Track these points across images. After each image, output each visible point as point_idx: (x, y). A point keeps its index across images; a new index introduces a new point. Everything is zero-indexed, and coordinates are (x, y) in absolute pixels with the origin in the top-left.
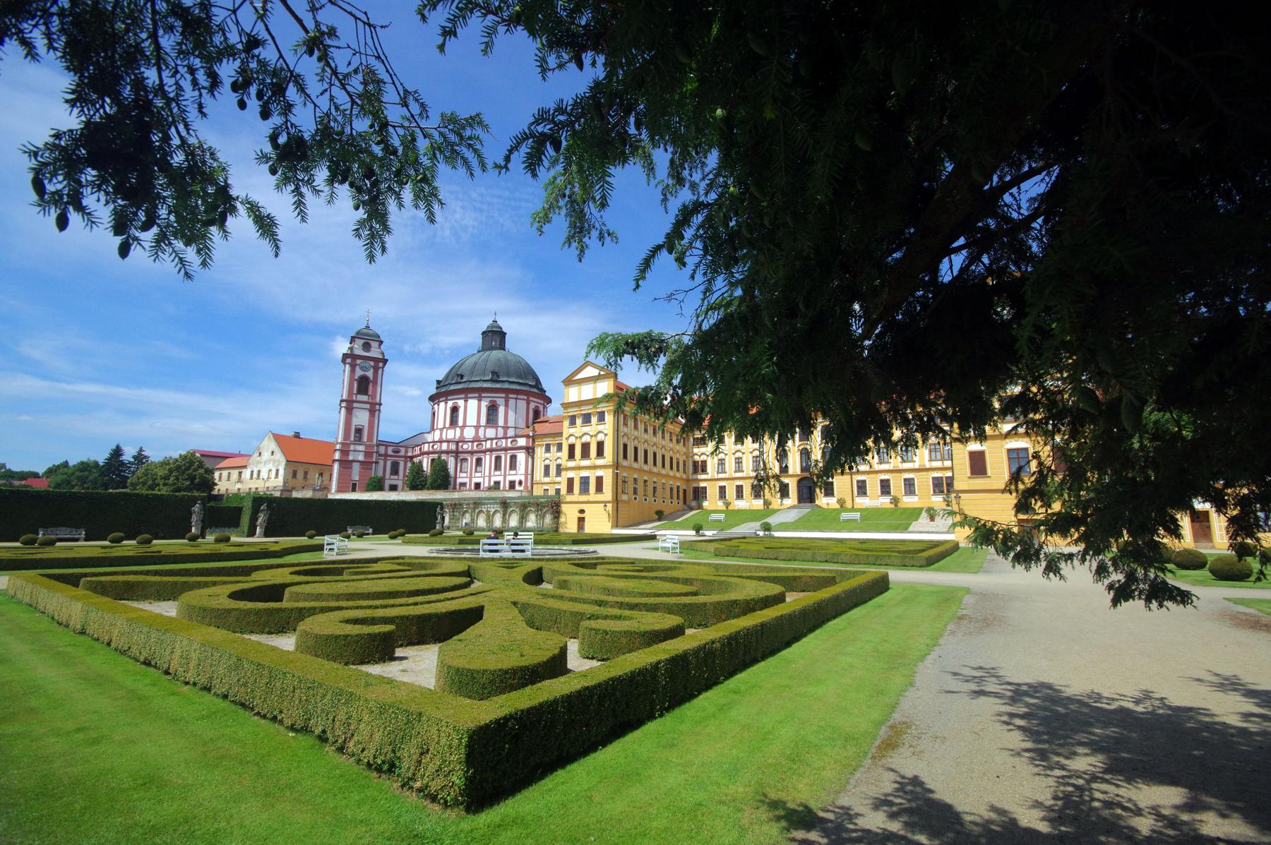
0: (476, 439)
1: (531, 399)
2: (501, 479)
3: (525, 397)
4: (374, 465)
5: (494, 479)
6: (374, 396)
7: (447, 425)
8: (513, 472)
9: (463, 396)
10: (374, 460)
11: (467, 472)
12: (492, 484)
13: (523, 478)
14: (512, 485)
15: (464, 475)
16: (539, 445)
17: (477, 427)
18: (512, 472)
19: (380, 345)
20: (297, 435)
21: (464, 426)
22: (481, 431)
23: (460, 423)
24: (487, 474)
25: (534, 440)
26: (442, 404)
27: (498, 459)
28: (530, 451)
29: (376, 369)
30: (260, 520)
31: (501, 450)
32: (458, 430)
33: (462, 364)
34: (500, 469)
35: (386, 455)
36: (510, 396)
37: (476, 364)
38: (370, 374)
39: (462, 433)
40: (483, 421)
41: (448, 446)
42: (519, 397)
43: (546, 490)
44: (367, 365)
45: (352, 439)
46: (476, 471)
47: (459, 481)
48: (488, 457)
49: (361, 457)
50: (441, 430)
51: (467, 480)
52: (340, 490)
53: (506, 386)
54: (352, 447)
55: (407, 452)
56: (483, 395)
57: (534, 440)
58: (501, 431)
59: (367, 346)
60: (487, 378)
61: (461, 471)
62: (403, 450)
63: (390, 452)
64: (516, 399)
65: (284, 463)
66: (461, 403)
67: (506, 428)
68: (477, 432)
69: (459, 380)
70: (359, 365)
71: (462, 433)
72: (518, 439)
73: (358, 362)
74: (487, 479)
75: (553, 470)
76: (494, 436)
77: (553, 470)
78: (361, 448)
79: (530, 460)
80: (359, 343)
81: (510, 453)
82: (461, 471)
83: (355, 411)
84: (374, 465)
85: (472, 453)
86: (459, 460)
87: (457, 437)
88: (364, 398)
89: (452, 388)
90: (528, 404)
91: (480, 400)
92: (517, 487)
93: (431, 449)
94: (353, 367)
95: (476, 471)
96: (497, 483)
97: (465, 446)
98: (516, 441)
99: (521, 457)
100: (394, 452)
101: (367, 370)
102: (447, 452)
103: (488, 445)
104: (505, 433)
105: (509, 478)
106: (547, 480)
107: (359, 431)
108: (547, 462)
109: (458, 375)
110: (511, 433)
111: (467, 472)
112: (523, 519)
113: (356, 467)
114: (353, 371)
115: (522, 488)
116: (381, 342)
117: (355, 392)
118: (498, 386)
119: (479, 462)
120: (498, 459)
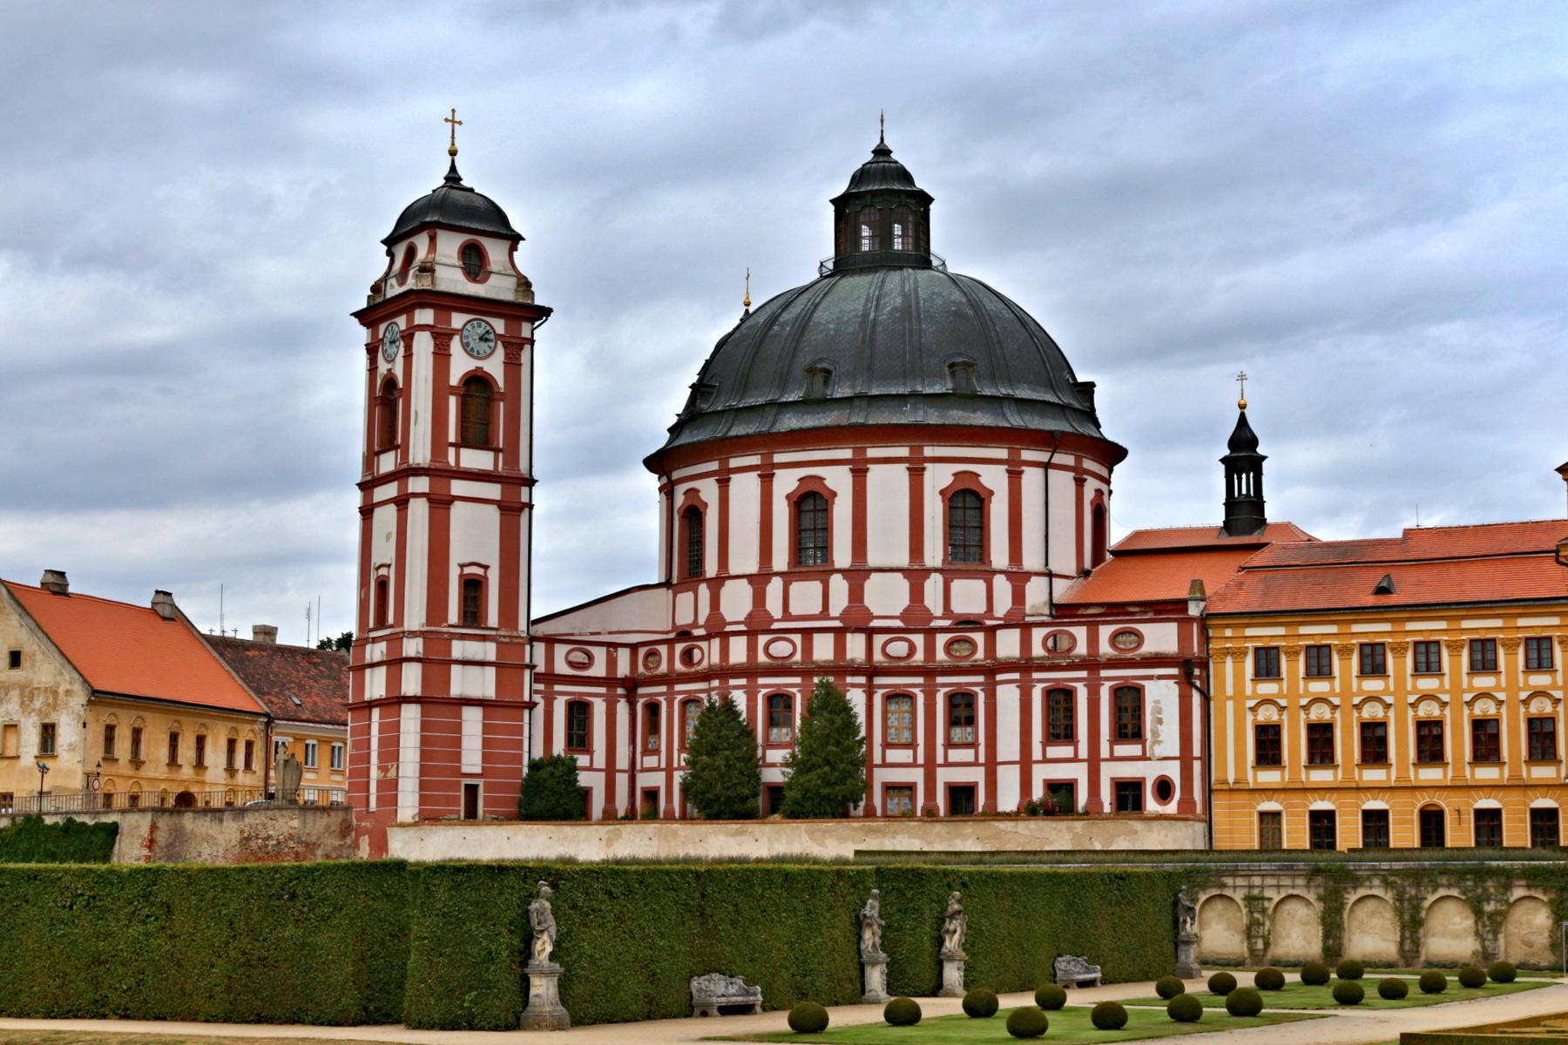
0: (915, 619)
1: (1088, 464)
2: (1079, 773)
3: (1069, 460)
4: (526, 712)
6: (511, 452)
7: (781, 561)
8: (1134, 749)
9: (847, 454)
10: (526, 698)
11: (912, 745)
12: (1038, 793)
13: (1173, 771)
14: (1129, 795)
15: (904, 755)
16: (1227, 652)
17: (916, 575)
18: (1122, 750)
19: (513, 248)
20: (56, 584)
21: (858, 575)
22: (933, 586)
23: (842, 556)
24: (1009, 747)
25: (1206, 639)
26: (745, 488)
27: (1060, 700)
29: (517, 347)
30: (952, 943)
32: (839, 585)
33: (804, 323)
35: (550, 678)
36: (1027, 455)
37: (868, 326)
38: (495, 367)
39: (856, 594)
40: (934, 553)
41: (840, 648)
42: (1060, 458)
43: (1270, 820)
45: (453, 615)
46: (950, 744)
47: (881, 776)
48: (1008, 695)
49: (483, 684)
50: (759, 580)
51: (917, 776)
52: (429, 817)
53: (1015, 420)
55: (612, 663)
56: (929, 451)
57: (1206, 639)
58: (1002, 586)
59: (474, 262)
60: (937, 389)
61: (887, 745)
62: (600, 654)
63: (561, 668)
64: (1047, 466)
65: (80, 697)
66: (839, 480)
67: (1019, 578)
68: (917, 594)
69: (818, 391)
70: (459, 332)
71: (856, 594)
73: (458, 320)
74: (1009, 779)
75: (1295, 744)
76: (979, 608)
77: (1295, 744)
78: (489, 651)
79: (1196, 698)
80: (449, 246)
81: (1111, 676)
82: (887, 745)
83: (457, 510)
84: (526, 712)
85: (929, 672)
86: (878, 699)
87: (836, 609)
89: (791, 422)
90: (1080, 483)
92: (1151, 805)
94: (442, 339)
95: (950, 744)
96: (1061, 791)
97: (898, 649)
99: (1161, 695)
100: (571, 664)
102: (841, 668)
103: (1008, 644)
104: (1019, 597)
106: (1270, 777)
107: (473, 587)
108: (1268, 715)
109: (811, 371)
110: (1036, 593)
111: (912, 745)
112: (1412, 924)
113: (472, 719)
114: (441, 356)
115: (1172, 808)
116: (515, 239)
117: (452, 438)
118: (981, 419)
119: (961, 710)
120: (1060, 700)
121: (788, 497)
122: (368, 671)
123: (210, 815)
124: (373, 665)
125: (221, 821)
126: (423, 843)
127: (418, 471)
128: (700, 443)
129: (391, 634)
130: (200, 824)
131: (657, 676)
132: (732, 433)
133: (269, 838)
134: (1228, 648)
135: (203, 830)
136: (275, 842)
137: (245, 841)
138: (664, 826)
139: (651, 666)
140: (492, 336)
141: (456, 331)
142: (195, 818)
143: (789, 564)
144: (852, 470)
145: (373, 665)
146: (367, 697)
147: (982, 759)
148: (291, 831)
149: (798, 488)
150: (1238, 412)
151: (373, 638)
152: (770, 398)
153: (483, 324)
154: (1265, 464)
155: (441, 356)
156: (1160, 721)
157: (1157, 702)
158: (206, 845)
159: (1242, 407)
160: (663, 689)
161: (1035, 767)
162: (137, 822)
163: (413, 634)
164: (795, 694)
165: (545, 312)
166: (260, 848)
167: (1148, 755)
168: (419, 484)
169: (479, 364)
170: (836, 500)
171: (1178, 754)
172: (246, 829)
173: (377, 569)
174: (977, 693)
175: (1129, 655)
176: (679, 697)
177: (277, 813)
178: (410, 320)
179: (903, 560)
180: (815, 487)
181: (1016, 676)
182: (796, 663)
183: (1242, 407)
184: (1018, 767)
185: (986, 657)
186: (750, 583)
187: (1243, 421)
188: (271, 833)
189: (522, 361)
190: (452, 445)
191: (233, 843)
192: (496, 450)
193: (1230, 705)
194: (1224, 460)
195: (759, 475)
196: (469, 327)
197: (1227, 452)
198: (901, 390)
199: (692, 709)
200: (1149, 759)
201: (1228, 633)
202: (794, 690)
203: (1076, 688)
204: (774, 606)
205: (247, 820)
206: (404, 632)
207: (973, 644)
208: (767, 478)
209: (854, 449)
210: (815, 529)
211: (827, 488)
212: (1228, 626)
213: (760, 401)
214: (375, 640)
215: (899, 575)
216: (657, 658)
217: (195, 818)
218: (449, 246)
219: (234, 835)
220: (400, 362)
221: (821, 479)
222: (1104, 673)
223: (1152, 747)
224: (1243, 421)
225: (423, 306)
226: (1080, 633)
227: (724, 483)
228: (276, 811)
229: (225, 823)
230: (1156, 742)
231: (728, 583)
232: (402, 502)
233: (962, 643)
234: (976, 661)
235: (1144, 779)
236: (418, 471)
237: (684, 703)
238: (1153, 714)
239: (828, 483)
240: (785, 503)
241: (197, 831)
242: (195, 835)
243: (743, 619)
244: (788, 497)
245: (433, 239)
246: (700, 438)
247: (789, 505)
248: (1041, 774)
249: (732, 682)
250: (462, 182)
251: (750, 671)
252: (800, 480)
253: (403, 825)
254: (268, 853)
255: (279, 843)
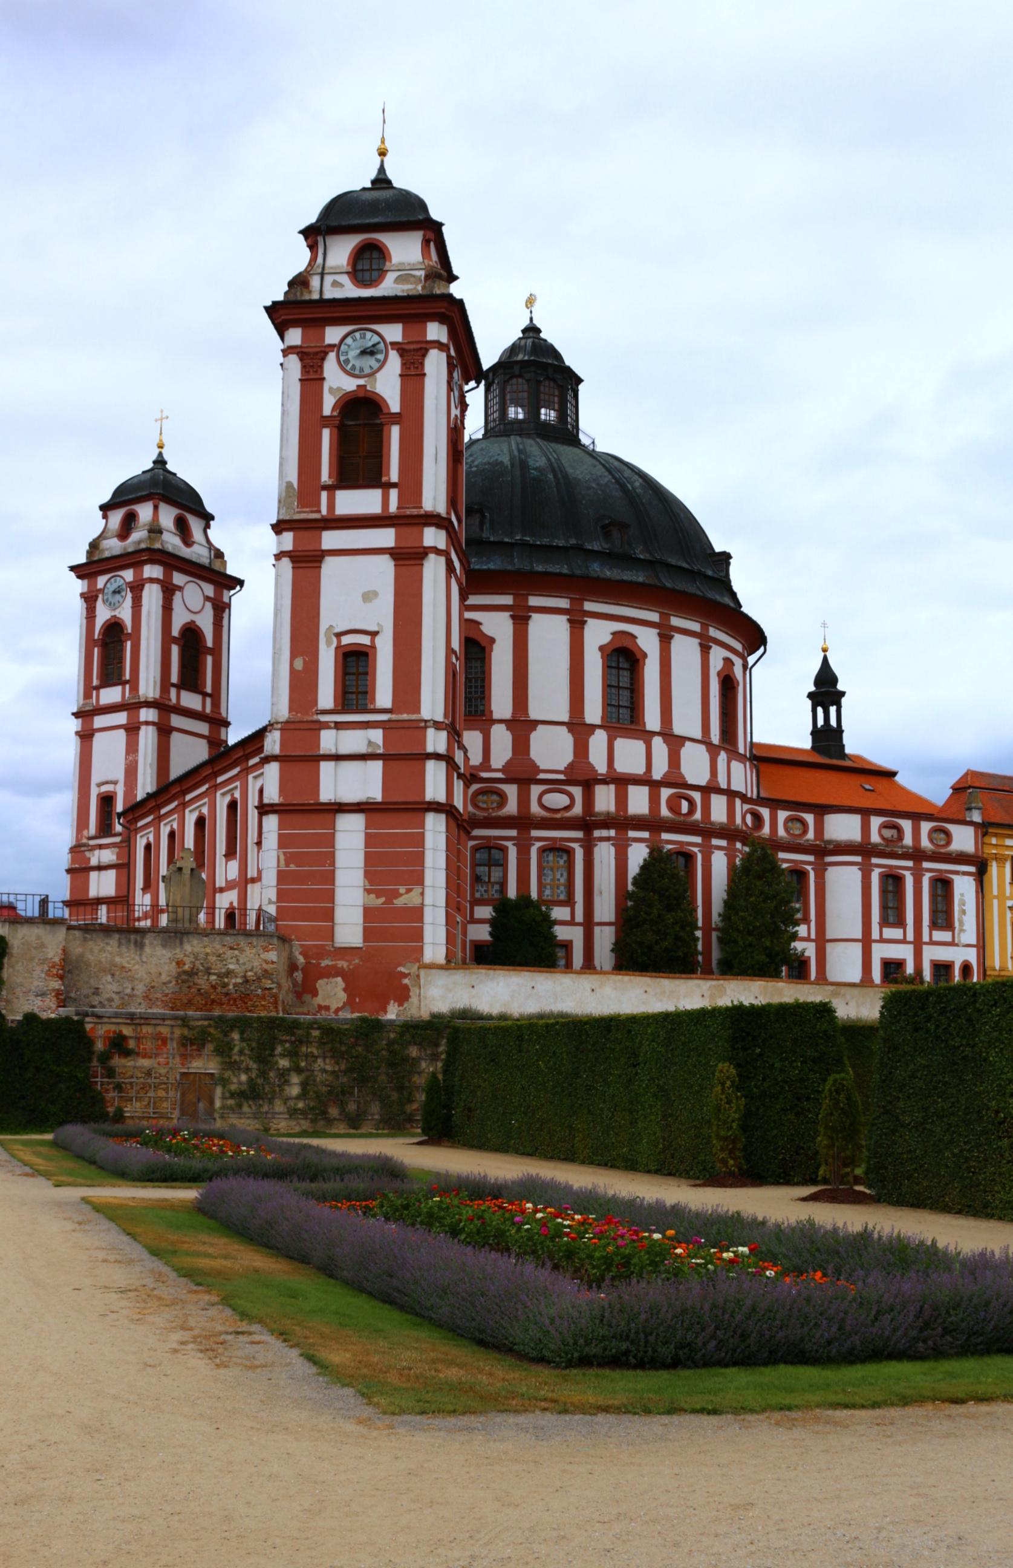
5: (880, 952)
7: (593, 713)
18: (940, 935)
23: (652, 720)
28: (981, 867)
31: (905, 856)
34: (901, 923)
39: (674, 760)
54: (328, 741)
57: (983, 843)
66: (648, 640)
71: (674, 760)
72: (952, 828)
91: (705, 650)
93: (665, 812)
98: (948, 834)
99: (964, 887)
105: (930, 954)
120: (893, 882)
121: (602, 648)
122: (326, 768)
123: (117, 936)
124: (338, 758)
125: (140, 946)
126: (474, 991)
128: (489, 571)
129: (389, 721)
130: (96, 949)
131: (499, 818)
132: (540, 568)
133: (229, 973)
134: (995, 854)
135: (104, 957)
136: (239, 980)
137: (186, 976)
138: (770, 984)
139: (485, 806)
142: (85, 940)
143: (603, 718)
144: (660, 635)
145: (338, 758)
146: (327, 794)
147: (813, 936)
148: (265, 966)
149: (612, 639)
150: (822, 654)
151: (336, 723)
152: (573, 541)
154: (844, 701)
156: (964, 912)
157: (962, 895)
158: (109, 978)
159: (825, 650)
160: (513, 833)
161: (874, 946)
162: (38, 937)
163: (438, 726)
164: (696, 854)
166: (214, 987)
167: (956, 942)
170: (647, 661)
171: (974, 943)
172: (187, 960)
173: (339, 635)
174: (809, 872)
175: (943, 850)
176: (539, 844)
177: (242, 941)
179: (698, 735)
180: (626, 643)
181: (858, 859)
182: (697, 821)
183: (825, 650)
184: (860, 944)
185: (816, 838)
186: (570, 731)
187: (825, 660)
188: (231, 967)
191: (164, 978)
193: (995, 902)
194: (811, 696)
195: (569, 620)
197: (812, 689)
198: (685, 565)
199: (551, 858)
200: (957, 945)
201: (994, 841)
202: (696, 850)
203: (904, 876)
204: (598, 759)
205: (188, 948)
206: (426, 721)
207: (804, 824)
208: (577, 625)
209: (661, 614)
210: (619, 687)
211: (638, 646)
212: (996, 835)
213: (561, 543)
214: (338, 726)
215: (703, 748)
216: (495, 797)
217: (85, 940)
219: (166, 967)
221: (634, 637)
222: (926, 865)
223: (959, 934)
224: (825, 660)
226: (906, 825)
227: (521, 619)
228: (241, 938)
229: (148, 950)
230: (962, 930)
231: (540, 727)
233: (795, 822)
234: (808, 840)
235: (953, 962)
237: (542, 851)
238: (959, 905)
239: (639, 642)
240: (599, 654)
241: (90, 957)
242: (88, 965)
243: (562, 769)
244: (602, 648)
246: (492, 566)
247: (602, 658)
248: (880, 952)
249: (632, 834)
251: (652, 824)
252: (614, 634)
253: (432, 966)
254: (227, 994)
255: (247, 981)
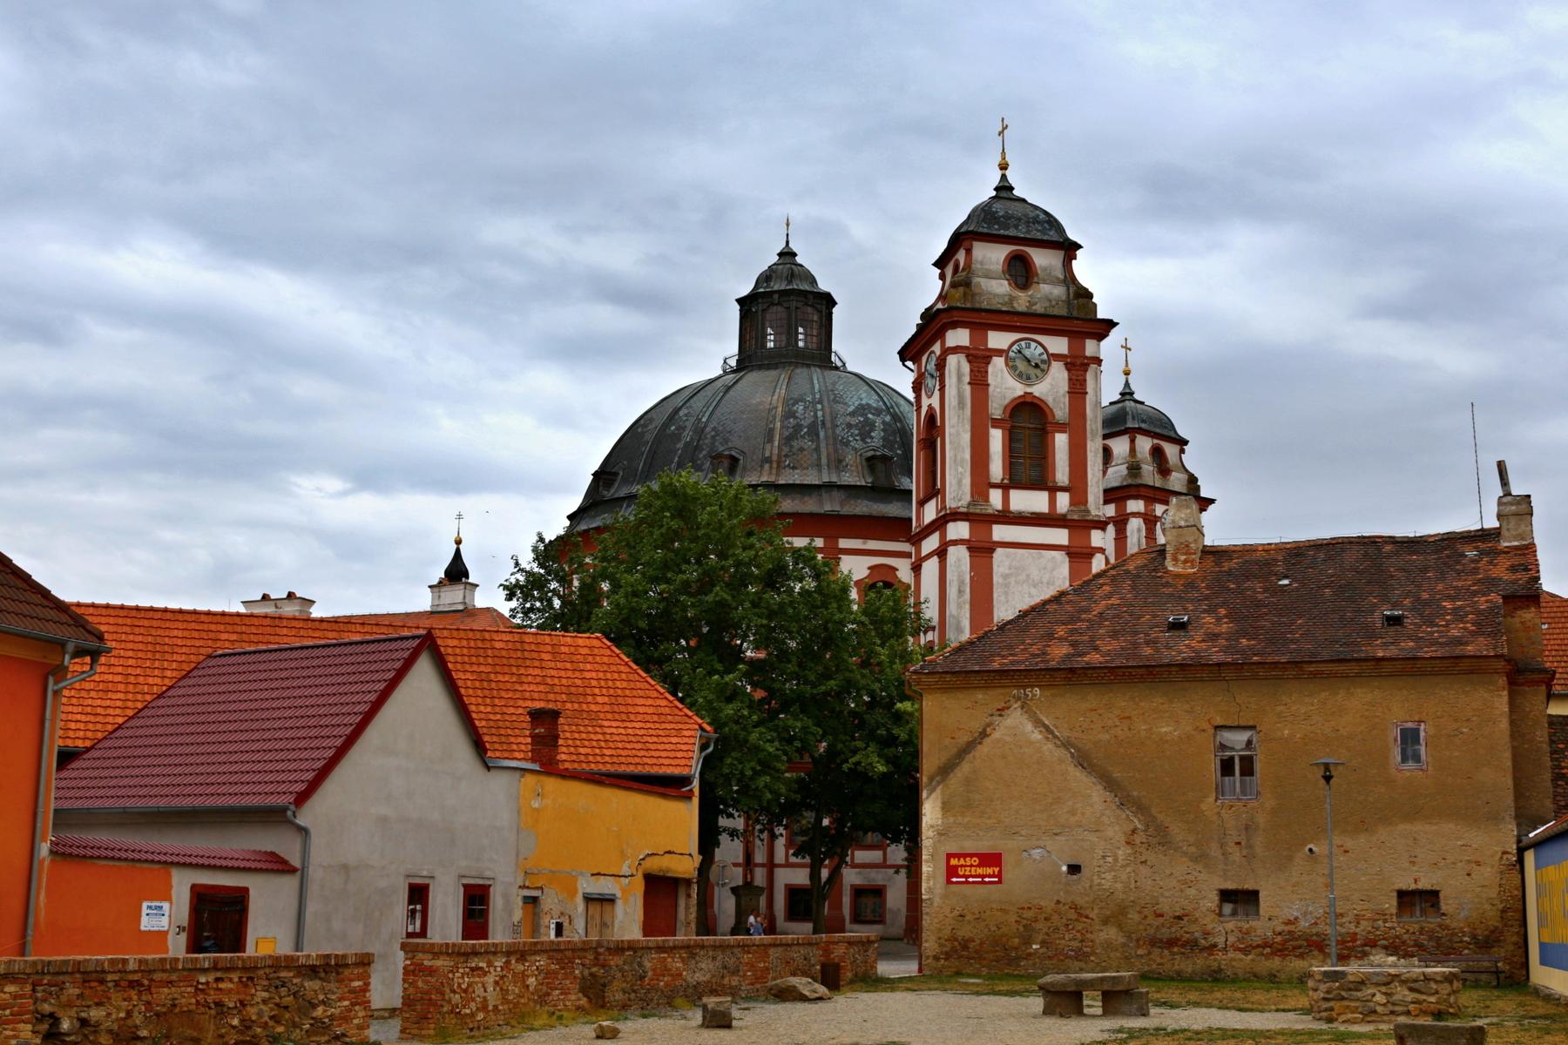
44: (1034, 351)
73: (998, 340)
80: (991, 256)
88: (1030, 501)
101: (1038, 368)
114: (979, 382)
127: (955, 516)
140: (1045, 357)
141: (999, 352)
153: (1033, 345)
155: (979, 382)
165: (1110, 324)
168: (959, 530)
169: (1029, 390)
178: (943, 343)
189: (1088, 390)
190: (996, 486)
192: (1053, 490)
196: (1015, 348)
218: (991, 256)
220: (937, 393)
225: (955, 325)
232: (941, 553)
236: (955, 516)
245: (969, 251)
250: (1014, 192)
